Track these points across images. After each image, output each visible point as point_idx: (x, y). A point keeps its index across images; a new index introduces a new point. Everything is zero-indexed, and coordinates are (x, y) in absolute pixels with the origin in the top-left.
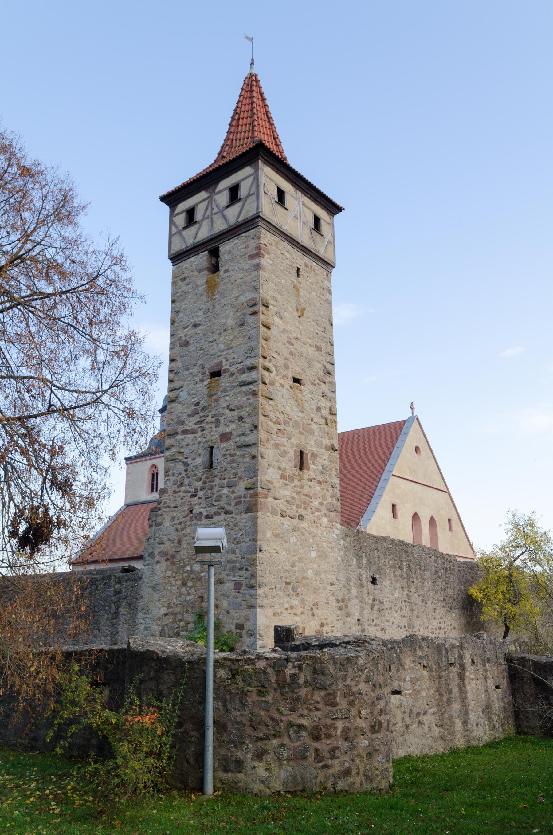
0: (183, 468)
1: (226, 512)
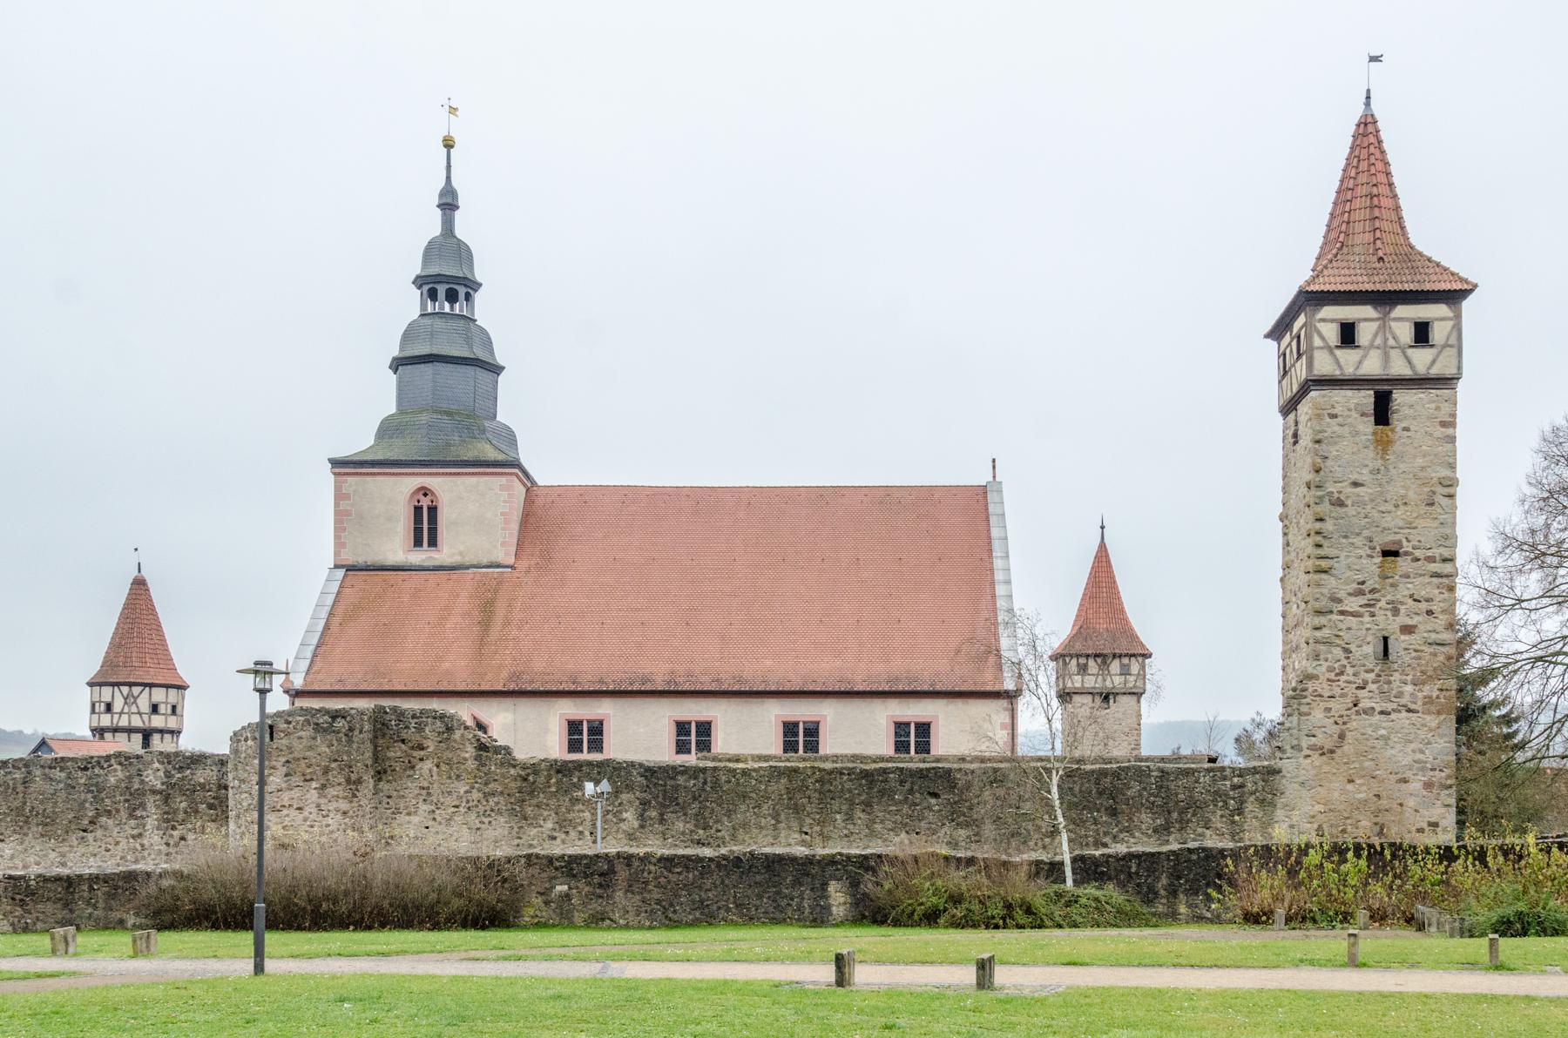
0: (1342, 655)
1: (1409, 711)
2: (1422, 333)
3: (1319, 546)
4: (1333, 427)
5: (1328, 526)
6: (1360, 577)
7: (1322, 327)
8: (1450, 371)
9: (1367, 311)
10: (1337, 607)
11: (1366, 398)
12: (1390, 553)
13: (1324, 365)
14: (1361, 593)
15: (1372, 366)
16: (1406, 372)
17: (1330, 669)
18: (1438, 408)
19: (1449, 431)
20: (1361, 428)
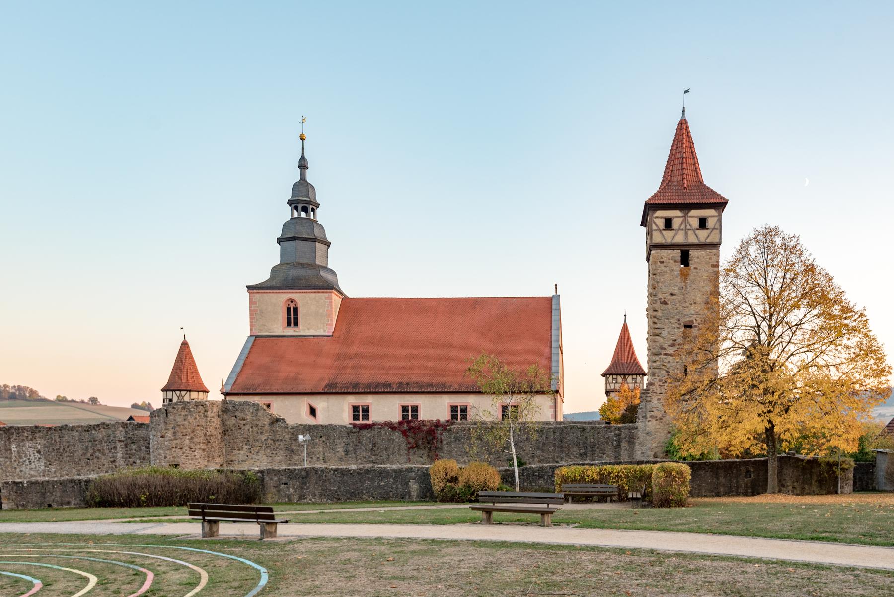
2: (703, 223)
3: (655, 323)
4: (662, 267)
5: (659, 314)
6: (674, 338)
7: (656, 220)
8: (716, 241)
9: (677, 213)
10: (663, 352)
11: (677, 253)
12: (688, 326)
13: (658, 239)
14: (673, 345)
15: (680, 239)
16: (695, 241)
17: (660, 381)
18: (710, 258)
19: (716, 269)
20: (675, 268)
